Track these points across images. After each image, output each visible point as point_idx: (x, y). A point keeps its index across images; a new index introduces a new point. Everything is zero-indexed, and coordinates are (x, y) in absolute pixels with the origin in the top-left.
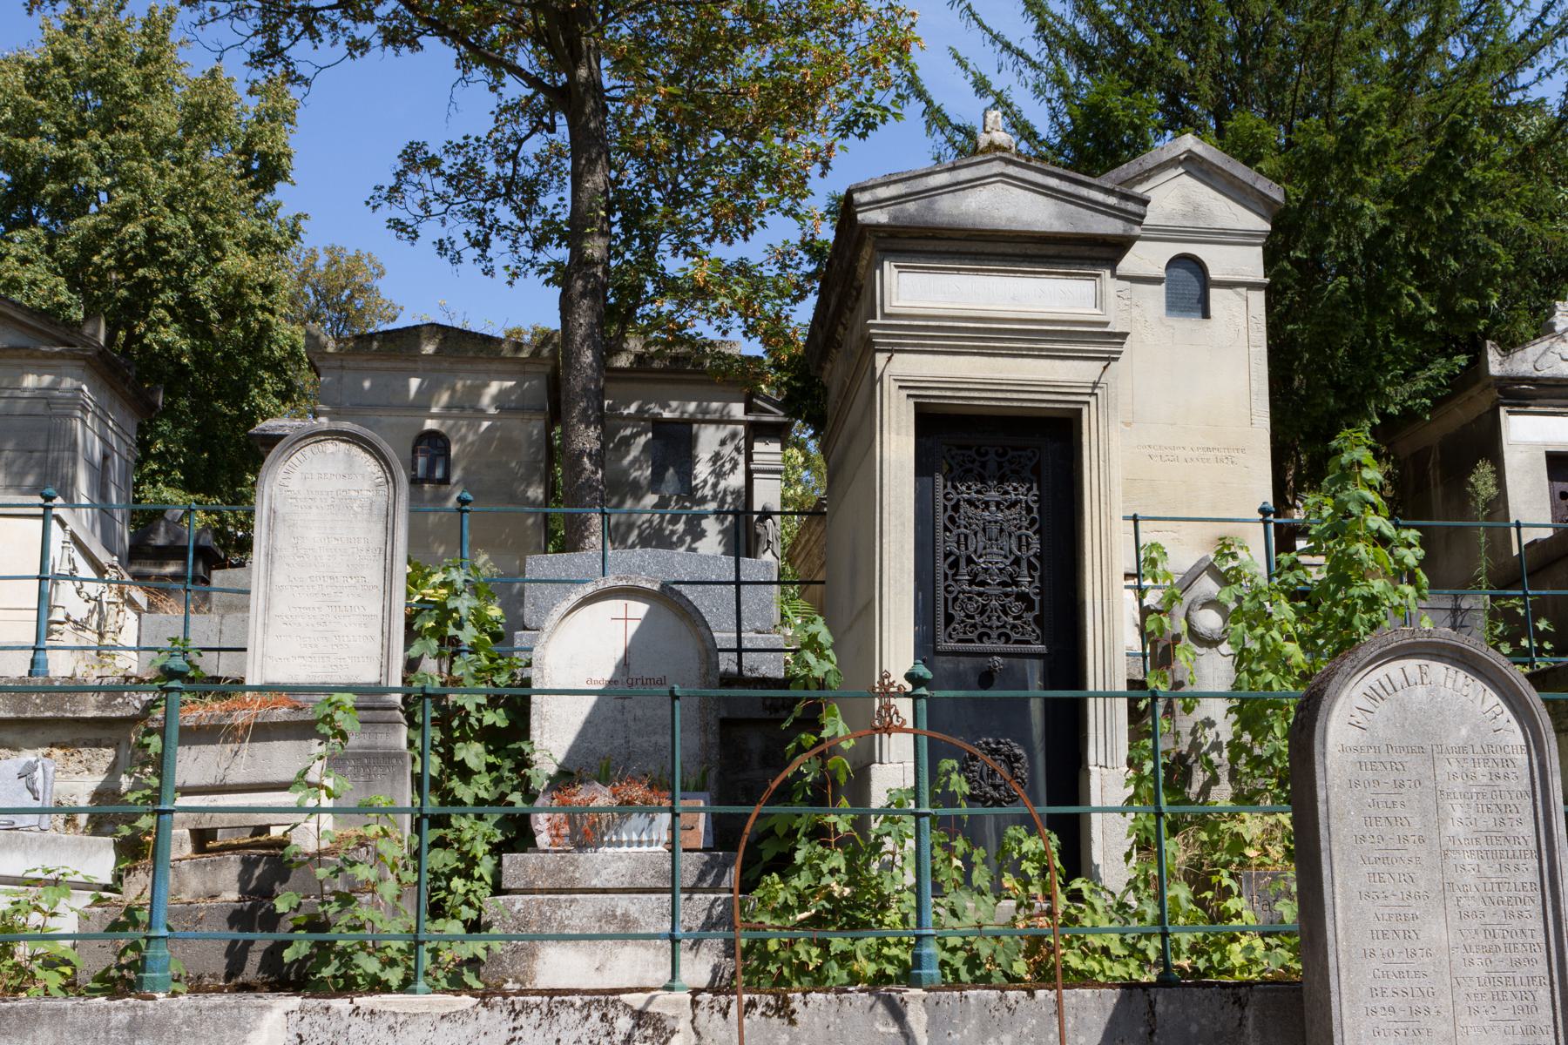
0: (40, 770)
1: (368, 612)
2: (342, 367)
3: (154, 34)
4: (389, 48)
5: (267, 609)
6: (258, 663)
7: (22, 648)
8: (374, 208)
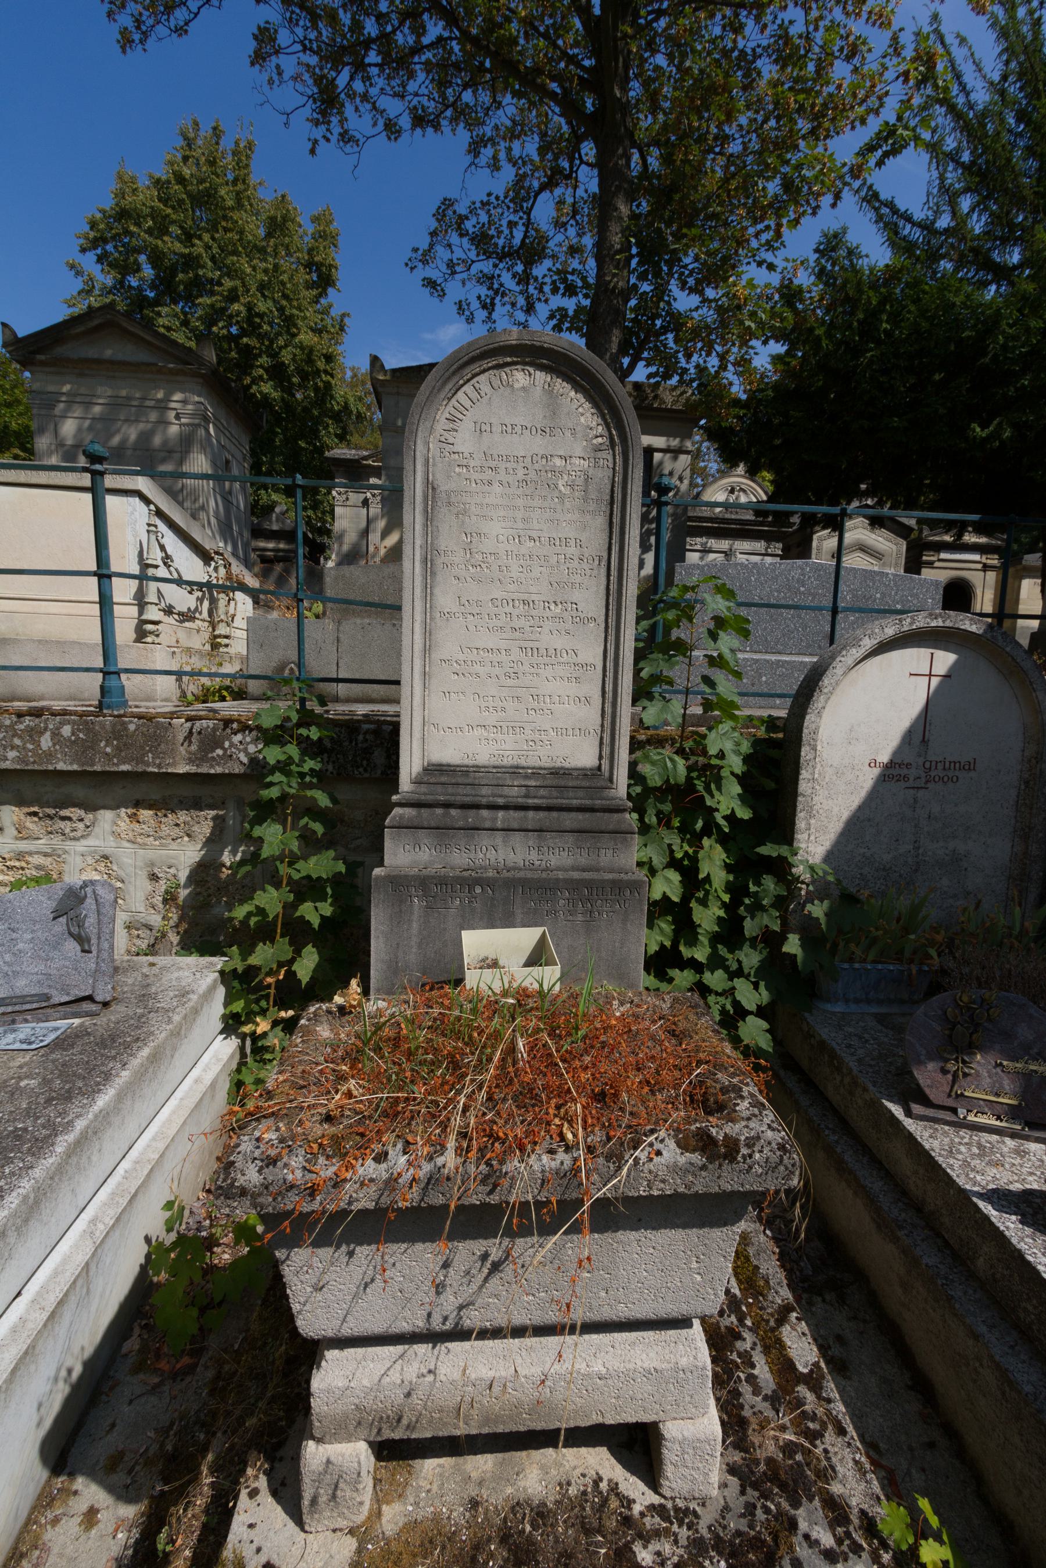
0: (90, 901)
1: (582, 658)
2: (398, 394)
3: (240, 160)
4: (419, 131)
5: (427, 650)
6: (417, 735)
7: (87, 670)
8: (412, 269)
